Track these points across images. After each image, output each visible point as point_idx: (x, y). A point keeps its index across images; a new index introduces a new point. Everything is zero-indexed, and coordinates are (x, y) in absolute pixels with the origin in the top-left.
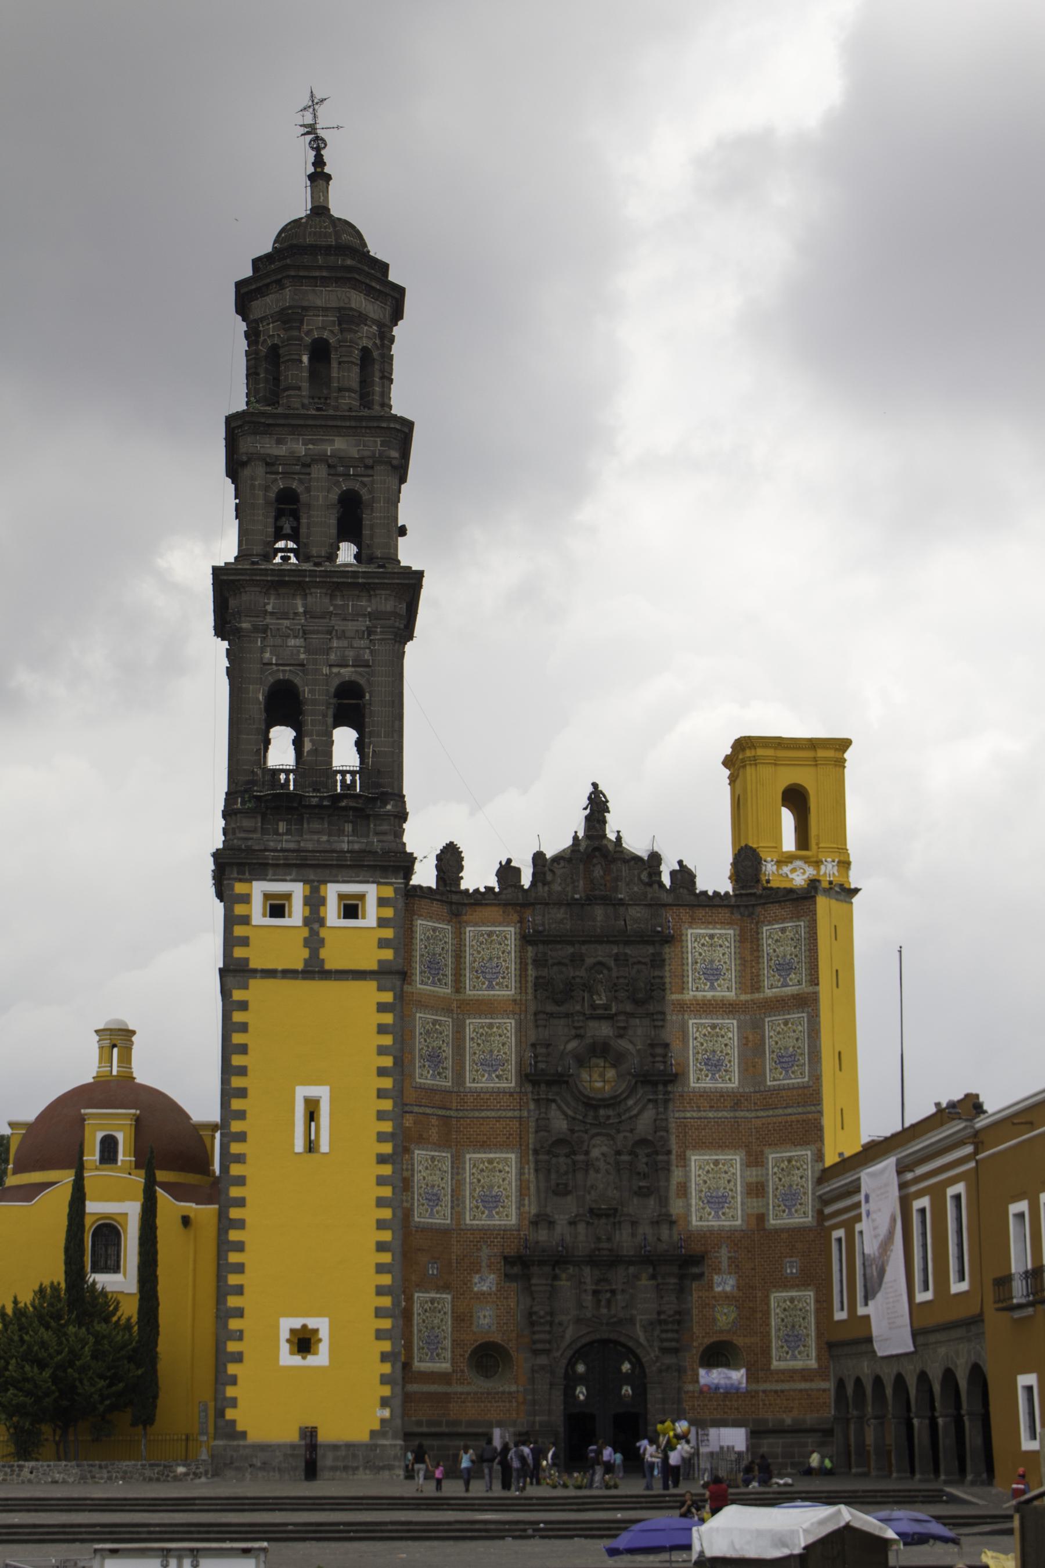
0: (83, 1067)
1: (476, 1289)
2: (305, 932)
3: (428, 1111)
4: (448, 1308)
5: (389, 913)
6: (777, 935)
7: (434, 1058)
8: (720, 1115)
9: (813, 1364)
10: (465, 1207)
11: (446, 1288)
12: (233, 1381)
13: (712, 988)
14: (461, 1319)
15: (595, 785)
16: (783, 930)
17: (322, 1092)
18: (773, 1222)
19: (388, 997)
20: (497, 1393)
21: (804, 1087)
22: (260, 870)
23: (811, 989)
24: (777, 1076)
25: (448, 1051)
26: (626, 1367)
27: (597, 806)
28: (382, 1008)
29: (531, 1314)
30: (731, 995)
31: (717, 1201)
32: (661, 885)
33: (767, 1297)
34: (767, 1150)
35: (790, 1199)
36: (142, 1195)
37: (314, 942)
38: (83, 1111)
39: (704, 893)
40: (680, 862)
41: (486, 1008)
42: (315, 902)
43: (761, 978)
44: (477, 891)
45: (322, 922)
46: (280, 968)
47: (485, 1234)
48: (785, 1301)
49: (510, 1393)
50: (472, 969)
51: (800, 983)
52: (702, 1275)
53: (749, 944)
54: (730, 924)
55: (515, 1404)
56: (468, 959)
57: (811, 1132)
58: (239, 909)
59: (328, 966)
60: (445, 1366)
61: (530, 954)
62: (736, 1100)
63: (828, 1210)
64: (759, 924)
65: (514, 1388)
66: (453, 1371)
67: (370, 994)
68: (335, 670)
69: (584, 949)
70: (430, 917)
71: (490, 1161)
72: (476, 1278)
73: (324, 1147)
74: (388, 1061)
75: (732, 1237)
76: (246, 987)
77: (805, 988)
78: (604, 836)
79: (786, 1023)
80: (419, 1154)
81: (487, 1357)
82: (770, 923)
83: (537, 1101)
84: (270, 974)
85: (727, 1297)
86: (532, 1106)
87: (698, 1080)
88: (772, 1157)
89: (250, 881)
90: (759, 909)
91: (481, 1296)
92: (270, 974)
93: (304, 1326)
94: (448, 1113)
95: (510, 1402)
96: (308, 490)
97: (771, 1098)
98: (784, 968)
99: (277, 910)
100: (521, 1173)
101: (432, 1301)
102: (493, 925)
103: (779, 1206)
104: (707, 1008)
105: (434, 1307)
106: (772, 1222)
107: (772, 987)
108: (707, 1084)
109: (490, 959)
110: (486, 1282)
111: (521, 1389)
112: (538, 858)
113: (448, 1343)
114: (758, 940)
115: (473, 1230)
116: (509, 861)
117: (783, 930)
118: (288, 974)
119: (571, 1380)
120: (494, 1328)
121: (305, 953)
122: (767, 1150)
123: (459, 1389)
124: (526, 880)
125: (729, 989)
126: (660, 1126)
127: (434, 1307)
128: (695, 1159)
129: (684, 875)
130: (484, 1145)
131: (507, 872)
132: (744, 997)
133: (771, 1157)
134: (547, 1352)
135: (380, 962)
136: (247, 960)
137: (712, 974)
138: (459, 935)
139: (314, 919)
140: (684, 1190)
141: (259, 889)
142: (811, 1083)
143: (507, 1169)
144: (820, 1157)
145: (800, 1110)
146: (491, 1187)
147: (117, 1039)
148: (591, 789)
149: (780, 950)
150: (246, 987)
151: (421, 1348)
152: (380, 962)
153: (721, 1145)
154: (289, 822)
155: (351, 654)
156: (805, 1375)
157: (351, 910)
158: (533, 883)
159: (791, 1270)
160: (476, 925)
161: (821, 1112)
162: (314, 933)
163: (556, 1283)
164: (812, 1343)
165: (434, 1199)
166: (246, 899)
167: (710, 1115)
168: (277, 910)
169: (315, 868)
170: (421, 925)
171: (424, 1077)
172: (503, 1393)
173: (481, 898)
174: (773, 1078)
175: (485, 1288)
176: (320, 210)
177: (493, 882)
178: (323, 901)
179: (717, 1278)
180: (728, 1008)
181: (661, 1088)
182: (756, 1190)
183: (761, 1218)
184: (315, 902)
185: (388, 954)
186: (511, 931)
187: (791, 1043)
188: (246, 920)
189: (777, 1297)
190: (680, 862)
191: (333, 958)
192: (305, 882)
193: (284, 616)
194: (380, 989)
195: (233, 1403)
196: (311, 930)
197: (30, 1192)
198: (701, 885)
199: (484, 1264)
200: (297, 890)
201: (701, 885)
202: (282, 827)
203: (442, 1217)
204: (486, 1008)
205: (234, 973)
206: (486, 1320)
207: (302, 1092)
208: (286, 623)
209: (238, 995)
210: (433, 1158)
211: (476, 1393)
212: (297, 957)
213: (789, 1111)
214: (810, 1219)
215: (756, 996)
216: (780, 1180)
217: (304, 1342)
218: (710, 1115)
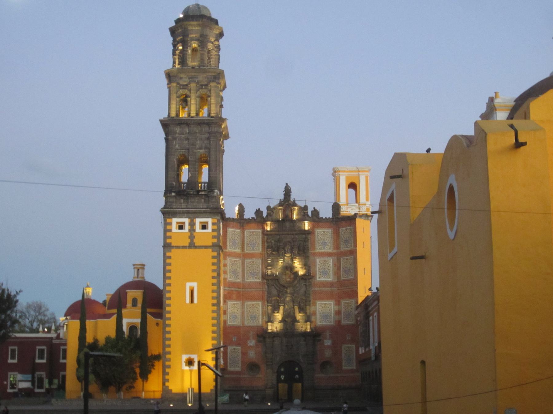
0: (130, 276)
2: (189, 234)
3: (232, 289)
4: (240, 351)
5: (215, 227)
6: (344, 231)
7: (234, 272)
8: (327, 289)
9: (354, 367)
11: (239, 344)
12: (168, 374)
13: (324, 248)
14: (244, 354)
15: (287, 184)
16: (346, 230)
17: (195, 285)
18: (343, 323)
19: (215, 254)
22: (175, 214)
25: (240, 270)
26: (297, 369)
27: (287, 191)
28: (213, 257)
29: (266, 353)
30: (331, 251)
31: (325, 317)
32: (308, 216)
36: (140, 317)
37: (192, 237)
39: (322, 218)
40: (314, 208)
41: (251, 256)
42: (192, 224)
44: (249, 219)
45: (194, 231)
46: (181, 245)
47: (251, 328)
50: (247, 244)
52: (320, 340)
53: (337, 234)
54: (329, 227)
56: (246, 240)
57: (355, 294)
58: (168, 227)
59: (196, 245)
60: (238, 369)
61: (266, 239)
62: (331, 284)
64: (339, 228)
67: (209, 253)
68: (198, 150)
69: (283, 236)
70: (233, 227)
71: (253, 305)
72: (249, 342)
74: (215, 274)
75: (331, 328)
76: (171, 252)
77: (352, 248)
78: (290, 200)
79: (347, 259)
80: (229, 303)
81: (253, 367)
82: (342, 227)
83: (268, 285)
84: (178, 247)
85: (329, 347)
86: (266, 287)
87: (319, 278)
88: (343, 302)
89: (172, 218)
92: (178, 247)
93: (190, 357)
94: (239, 290)
98: (347, 242)
99: (181, 227)
100: (263, 309)
101: (234, 349)
102: (254, 229)
104: (322, 255)
105: (235, 351)
107: (343, 248)
108: (322, 279)
109: (253, 240)
110: (252, 343)
112: (268, 208)
113: (240, 362)
116: (259, 209)
117: (346, 230)
118: (184, 247)
119: (279, 373)
121: (189, 241)
124: (265, 215)
125: (330, 249)
126: (306, 293)
127: (235, 351)
128: (319, 303)
129: (316, 212)
130: (251, 300)
131: (258, 212)
135: (213, 243)
136: (171, 243)
137: (324, 244)
138: (243, 233)
139: (192, 230)
140: (315, 313)
141: (175, 221)
144: (357, 302)
147: (140, 268)
148: (285, 185)
150: (171, 252)
151: (230, 364)
152: (213, 243)
153: (328, 299)
154: (184, 199)
155: (204, 145)
156: (352, 371)
157: (204, 227)
158: (267, 216)
159: (348, 338)
160: (248, 229)
164: (354, 361)
165: (235, 317)
166: (171, 224)
168: (181, 227)
169: (192, 215)
170: (230, 230)
171: (231, 278)
173: (249, 221)
177: (254, 216)
178: (195, 224)
179: (325, 341)
180: (330, 255)
181: (308, 281)
182: (338, 313)
183: (339, 322)
184: (192, 224)
185: (215, 241)
186: (260, 231)
188: (170, 231)
189: (344, 347)
190: (314, 208)
191: (197, 242)
192: (189, 218)
193: (182, 134)
194: (212, 251)
195: (168, 381)
197: (108, 316)
198: (321, 216)
200: (186, 221)
201: (321, 215)
202: (182, 201)
203: (238, 323)
204: (251, 256)
205: (167, 246)
206: (252, 354)
207: (189, 285)
208: (183, 136)
209: (168, 254)
210: (234, 304)
212: (187, 242)
217: (190, 362)
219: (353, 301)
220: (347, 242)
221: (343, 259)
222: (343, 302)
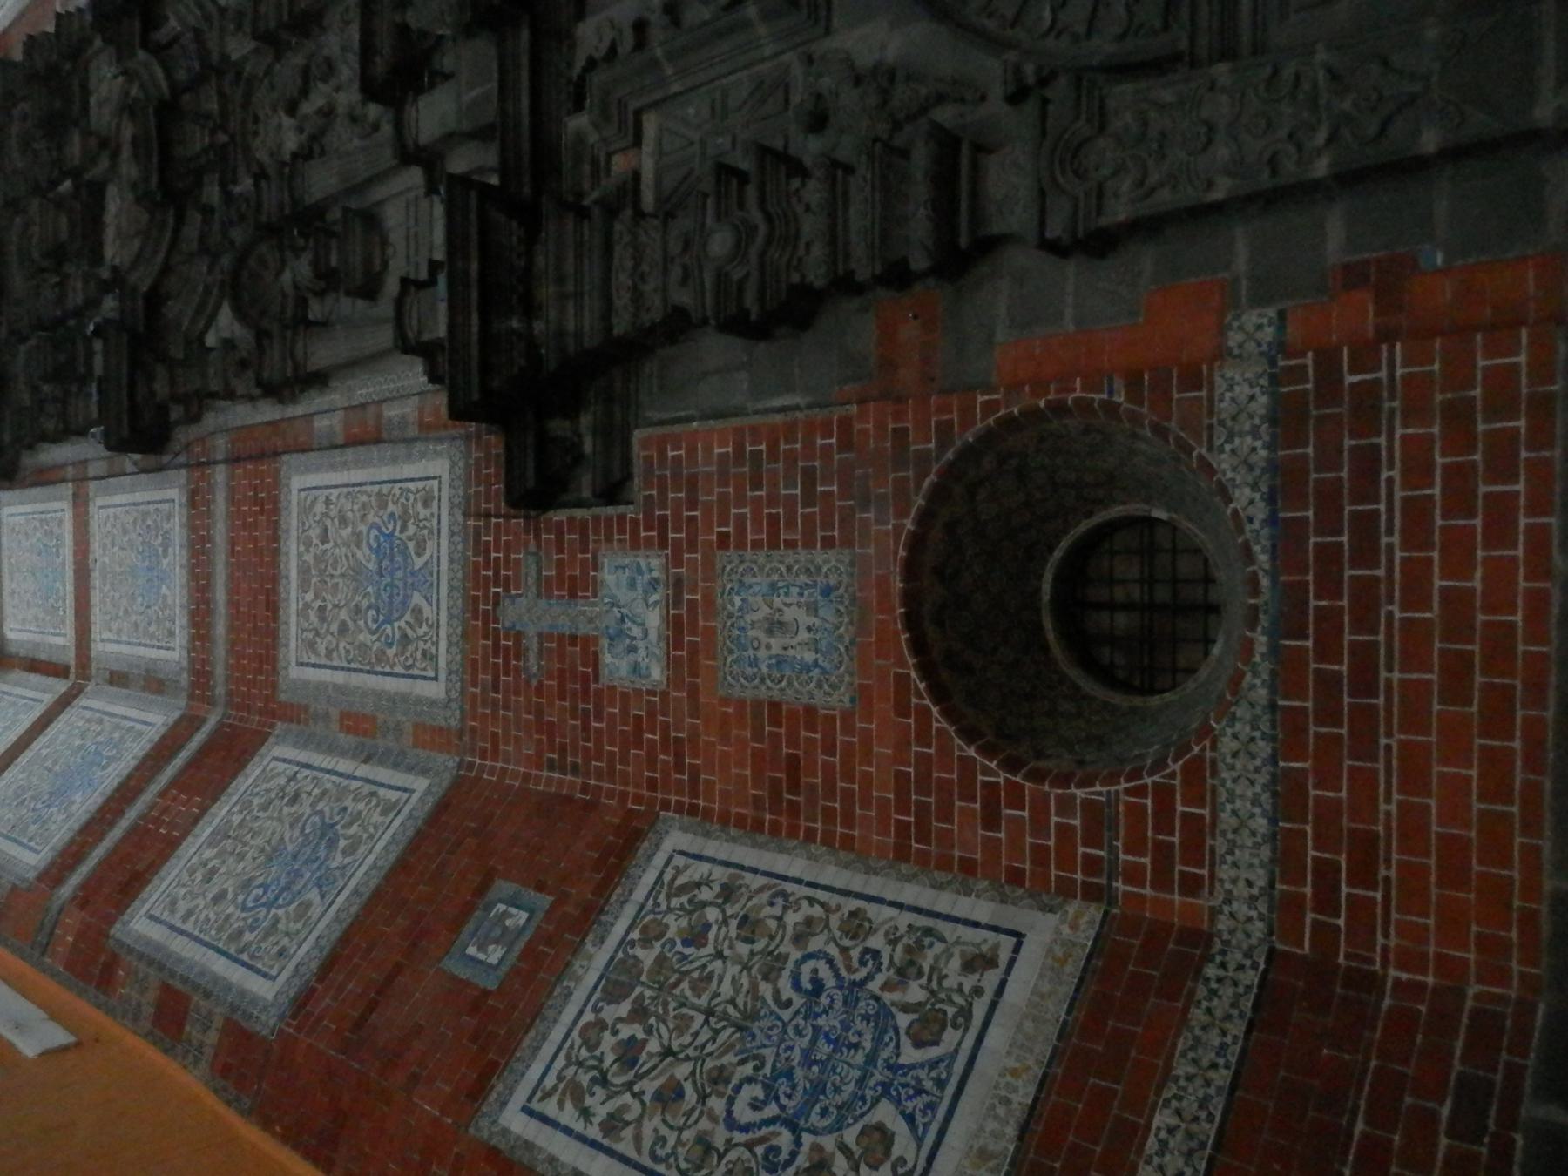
1: (657, 674)
10: (405, 698)
20: (1287, 538)
49: (1287, 419)
55: (1396, 363)
65: (1241, 391)
66: (1092, 893)
91: (688, 633)
95: (1367, 407)
111: (1254, 327)
115: (471, 667)
120: (832, 563)
123: (1241, 875)
134: (956, 159)
143: (320, 508)
146: (357, 570)
163: (648, 199)
172: (1285, 483)
175: (654, 619)
199: (559, 616)
211: (1288, 732)
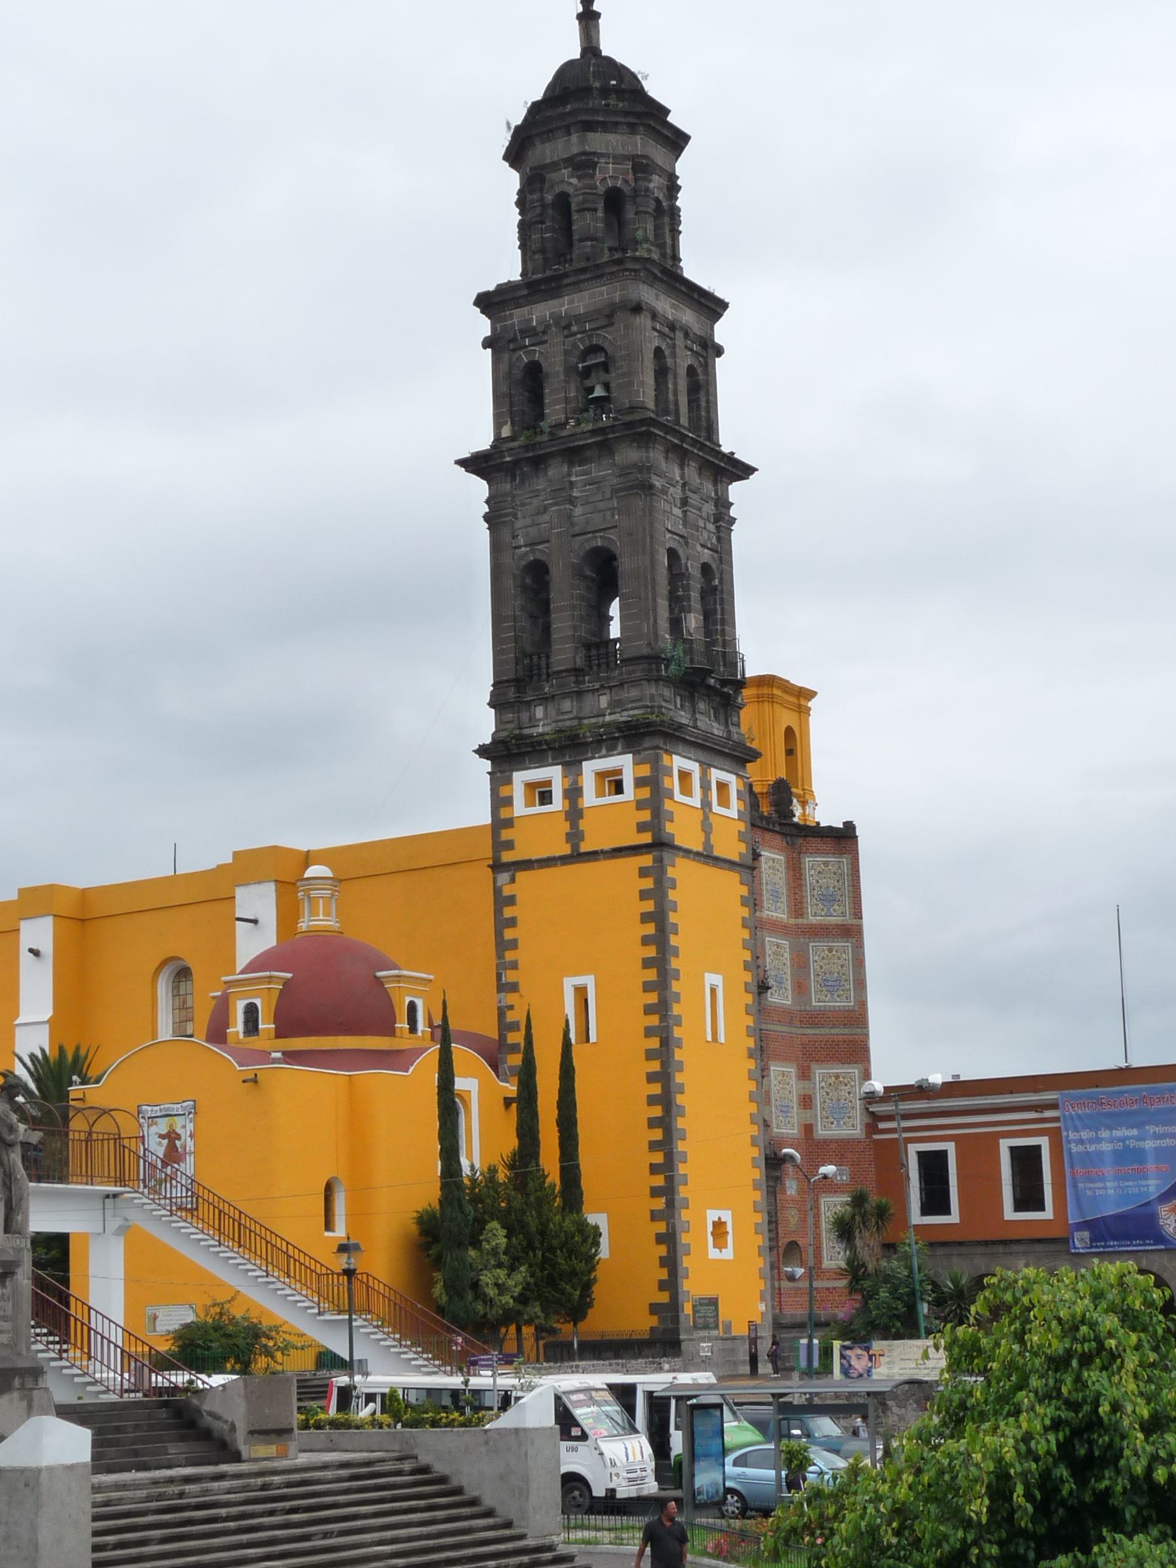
16: (826, 864)
18: (821, 1132)
21: (849, 1011)
23: (854, 922)
24: (822, 998)
33: (817, 1201)
34: (814, 1066)
35: (838, 1112)
37: (707, 827)
38: (379, 974)
43: (805, 905)
48: (835, 1205)
51: (843, 914)
53: (795, 871)
59: (716, 853)
63: (882, 1126)
73: (722, 1039)
77: (848, 920)
79: (830, 950)
88: (818, 1072)
90: (800, 841)
92: (687, 852)
96: (674, 355)
97: (815, 1019)
98: (828, 899)
103: (827, 1118)
106: (821, 1132)
107: (815, 915)
114: (800, 869)
122: (814, 1066)
132: (792, 921)
133: (818, 1072)
139: (706, 804)
142: (857, 1008)
145: (846, 1031)
149: (823, 882)
161: (867, 1035)
162: (706, 818)
167: (779, 1028)
174: (818, 1001)
176: (590, 48)
179: (788, 1183)
182: (806, 1102)
184: (705, 787)
187: (836, 969)
196: (705, 813)
213: (835, 1031)
214: (858, 1131)
215: (800, 921)
216: (828, 1093)
218: (779, 1028)
219: (855, 1071)
220: (828, 899)
221: (817, 951)
222: (818, 1072)
